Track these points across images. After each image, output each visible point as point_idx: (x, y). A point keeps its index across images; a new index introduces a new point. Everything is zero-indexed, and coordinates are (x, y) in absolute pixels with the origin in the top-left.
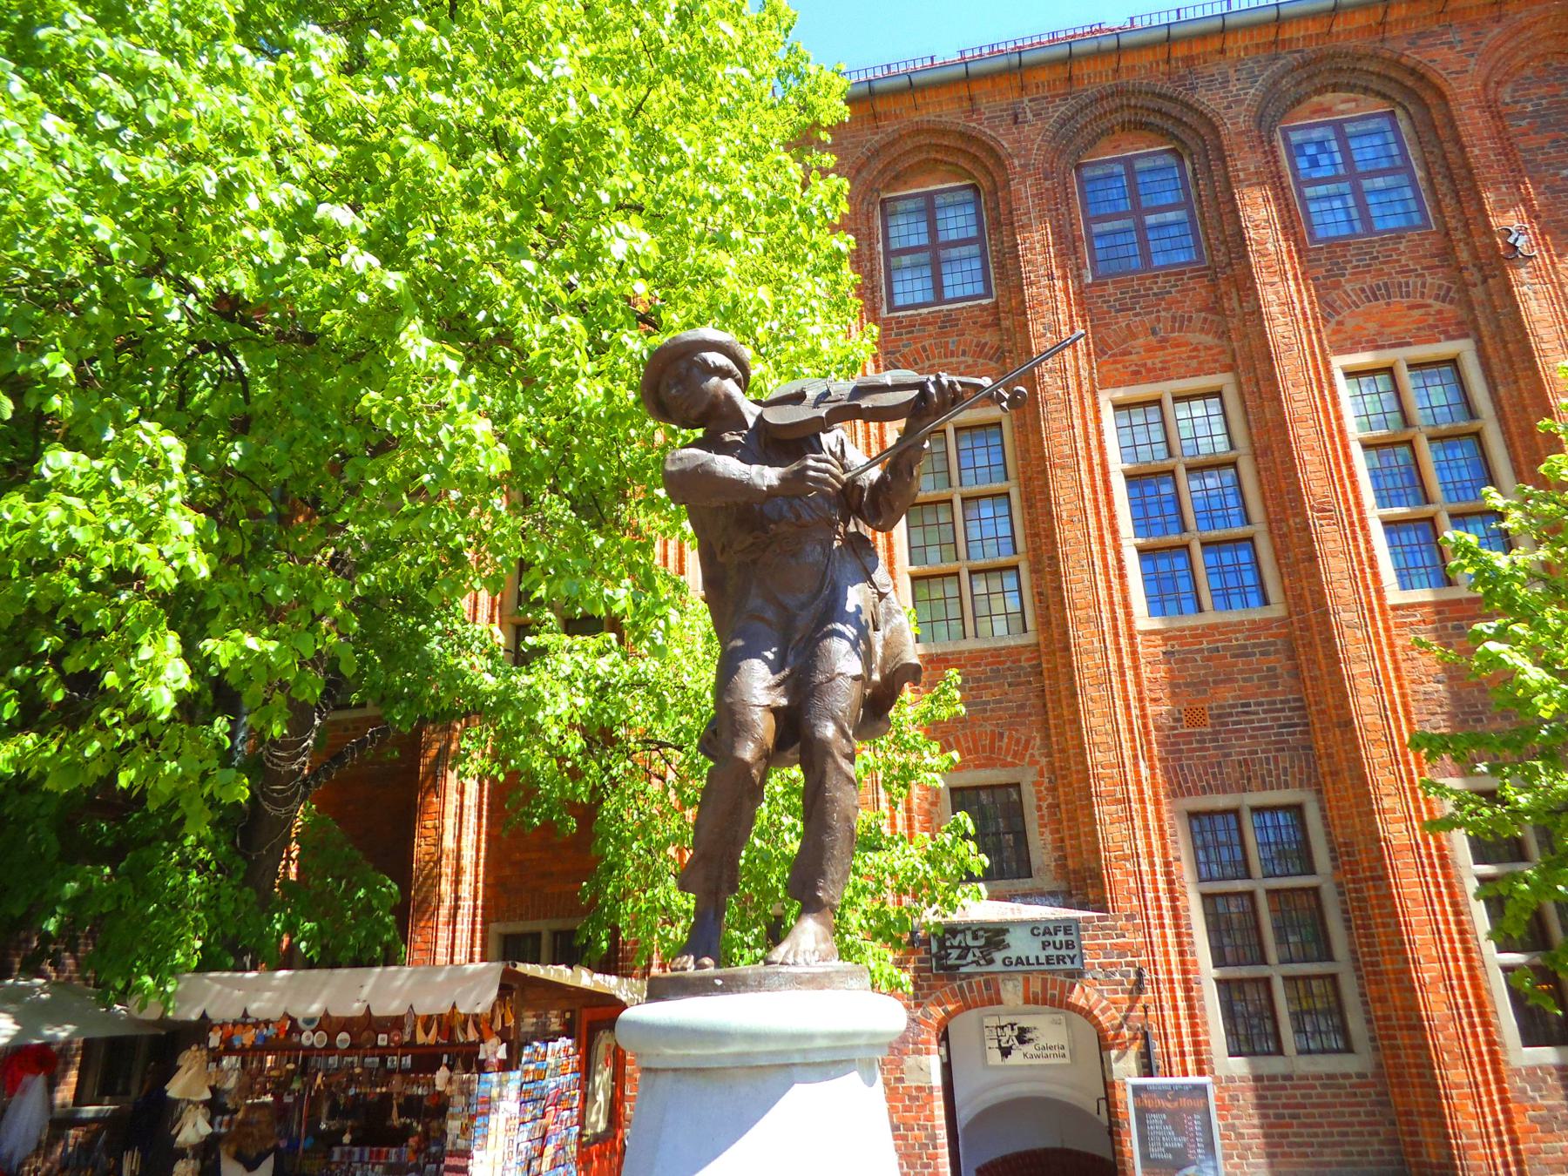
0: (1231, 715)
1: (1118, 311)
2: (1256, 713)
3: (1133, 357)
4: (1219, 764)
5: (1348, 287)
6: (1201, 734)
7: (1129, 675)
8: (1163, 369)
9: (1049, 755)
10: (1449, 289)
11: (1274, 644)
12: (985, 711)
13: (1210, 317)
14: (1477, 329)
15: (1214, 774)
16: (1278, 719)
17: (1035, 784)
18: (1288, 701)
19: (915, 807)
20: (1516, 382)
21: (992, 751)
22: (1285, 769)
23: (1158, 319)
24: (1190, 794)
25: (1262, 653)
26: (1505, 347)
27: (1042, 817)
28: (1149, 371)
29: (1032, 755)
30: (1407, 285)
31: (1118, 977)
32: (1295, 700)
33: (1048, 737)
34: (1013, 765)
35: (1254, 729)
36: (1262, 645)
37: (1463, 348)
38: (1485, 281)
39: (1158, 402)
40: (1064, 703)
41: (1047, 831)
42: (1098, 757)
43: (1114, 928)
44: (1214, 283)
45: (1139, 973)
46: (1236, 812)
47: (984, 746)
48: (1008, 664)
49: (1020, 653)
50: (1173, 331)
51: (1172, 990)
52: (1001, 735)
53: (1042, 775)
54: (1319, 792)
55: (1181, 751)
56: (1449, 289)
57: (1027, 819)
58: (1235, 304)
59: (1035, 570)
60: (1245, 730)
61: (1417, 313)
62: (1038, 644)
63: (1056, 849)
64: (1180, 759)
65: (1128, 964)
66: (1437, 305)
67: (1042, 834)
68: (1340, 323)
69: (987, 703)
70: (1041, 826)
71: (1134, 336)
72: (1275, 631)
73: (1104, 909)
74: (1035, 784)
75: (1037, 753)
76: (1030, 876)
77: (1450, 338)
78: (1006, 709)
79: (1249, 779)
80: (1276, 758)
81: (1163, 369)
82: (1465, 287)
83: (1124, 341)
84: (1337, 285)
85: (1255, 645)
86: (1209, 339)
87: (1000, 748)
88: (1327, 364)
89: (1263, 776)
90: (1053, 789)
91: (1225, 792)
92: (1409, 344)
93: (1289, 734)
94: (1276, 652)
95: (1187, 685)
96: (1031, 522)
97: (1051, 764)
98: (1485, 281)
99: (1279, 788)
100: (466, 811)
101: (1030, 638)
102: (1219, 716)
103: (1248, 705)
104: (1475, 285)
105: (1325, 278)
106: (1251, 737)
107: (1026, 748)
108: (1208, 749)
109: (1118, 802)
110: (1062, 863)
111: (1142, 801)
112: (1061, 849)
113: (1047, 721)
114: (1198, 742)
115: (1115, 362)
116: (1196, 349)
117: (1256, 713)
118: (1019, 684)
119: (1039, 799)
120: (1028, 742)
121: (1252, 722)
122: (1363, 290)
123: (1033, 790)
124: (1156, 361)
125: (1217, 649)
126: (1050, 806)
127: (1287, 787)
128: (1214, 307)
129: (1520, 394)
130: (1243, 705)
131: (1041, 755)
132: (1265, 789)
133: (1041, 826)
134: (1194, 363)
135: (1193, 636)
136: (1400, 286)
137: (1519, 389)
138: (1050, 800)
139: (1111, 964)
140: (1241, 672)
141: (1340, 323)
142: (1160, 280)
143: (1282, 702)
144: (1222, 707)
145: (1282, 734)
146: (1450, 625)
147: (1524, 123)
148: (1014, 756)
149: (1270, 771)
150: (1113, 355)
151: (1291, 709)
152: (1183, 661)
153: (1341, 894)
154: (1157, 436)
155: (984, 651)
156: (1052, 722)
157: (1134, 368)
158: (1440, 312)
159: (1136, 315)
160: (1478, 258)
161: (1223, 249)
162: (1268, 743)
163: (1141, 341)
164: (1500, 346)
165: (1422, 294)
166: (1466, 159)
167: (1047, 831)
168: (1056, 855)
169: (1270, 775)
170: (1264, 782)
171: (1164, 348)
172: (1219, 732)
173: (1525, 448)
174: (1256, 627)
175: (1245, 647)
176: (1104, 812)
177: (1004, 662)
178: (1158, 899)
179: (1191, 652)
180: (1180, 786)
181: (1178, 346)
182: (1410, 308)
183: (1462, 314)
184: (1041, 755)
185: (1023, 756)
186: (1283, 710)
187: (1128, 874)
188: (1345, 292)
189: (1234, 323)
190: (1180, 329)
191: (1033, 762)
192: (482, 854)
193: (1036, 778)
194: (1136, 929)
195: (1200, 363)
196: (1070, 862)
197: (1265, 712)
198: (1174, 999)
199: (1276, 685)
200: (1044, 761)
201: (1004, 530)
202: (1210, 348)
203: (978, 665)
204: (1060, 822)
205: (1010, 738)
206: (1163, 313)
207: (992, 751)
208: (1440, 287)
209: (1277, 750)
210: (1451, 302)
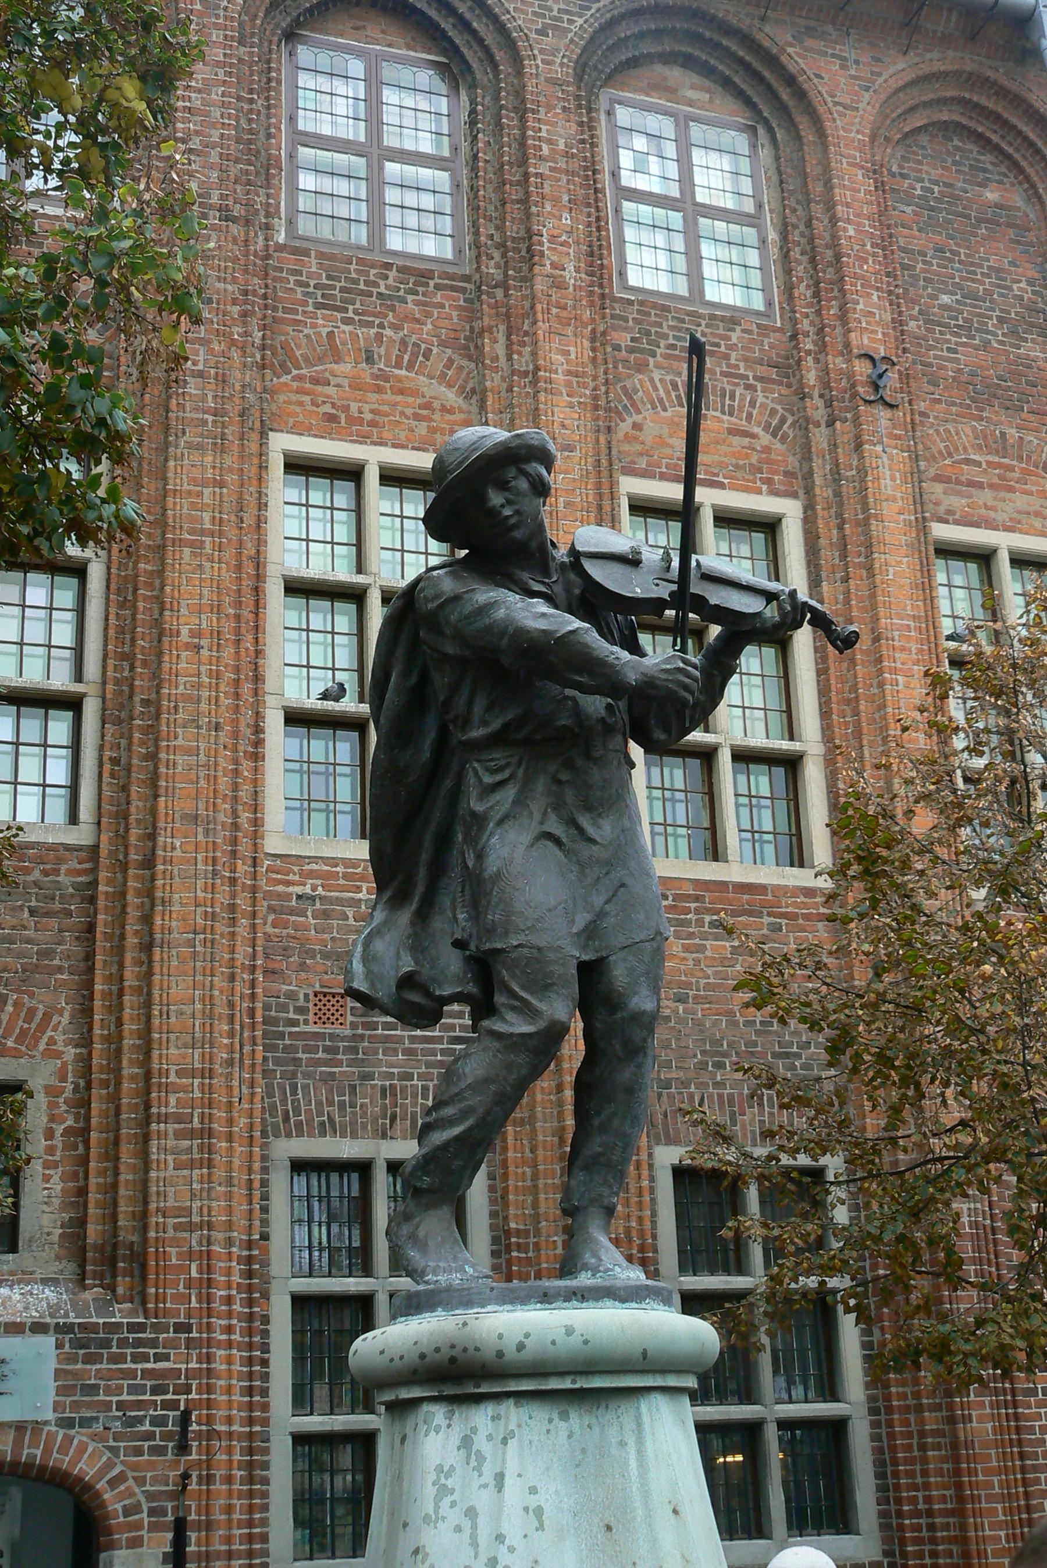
1: (318, 306)
3: (330, 390)
4: (353, 1088)
5: (657, 375)
6: (333, 1037)
8: (372, 424)
10: (783, 420)
13: (460, 361)
14: (809, 491)
15: (342, 1104)
17: (52, 1092)
20: (846, 580)
23: (379, 337)
24: (300, 1134)
26: (840, 527)
27: (50, 1150)
28: (352, 420)
29: (52, 1041)
30: (732, 397)
31: (147, 1427)
34: (17, 1055)
37: (790, 511)
38: (831, 423)
39: (353, 473)
40: (129, 956)
42: (172, 1055)
43: (153, 1343)
44: (471, 312)
45: (185, 1419)
46: (363, 1168)
48: (36, 875)
49: (60, 860)
50: (398, 365)
53: (63, 1079)
55: (297, 1062)
56: (783, 420)
58: (500, 350)
60: (399, 1040)
61: (737, 441)
62: (95, 849)
63: (64, 1206)
64: (294, 1075)
66: (765, 439)
67: (47, 1178)
68: (636, 426)
71: (338, 360)
75: (60, 1038)
76: (13, 1249)
77: (774, 492)
78: (21, 955)
81: (372, 424)
82: (804, 424)
83: (321, 360)
84: (642, 367)
86: (452, 397)
88: (613, 484)
91: (354, 1136)
92: (721, 486)
95: (326, 956)
96: (120, 630)
98: (831, 423)
101: (81, 835)
104: (818, 425)
105: (631, 350)
106: (407, 1052)
107: (42, 1028)
108: (339, 1064)
109: (192, 1134)
113: (89, 985)
114: (326, 1049)
115: (300, 391)
116: (427, 406)
118: (48, 914)
119: (52, 1119)
120: (47, 1017)
122: (675, 386)
124: (363, 407)
126: (67, 1132)
128: (471, 348)
129: (847, 601)
134: (422, 428)
135: (346, 876)
136: (723, 395)
137: (847, 593)
138: (70, 1122)
139: (139, 1405)
141: (636, 426)
142: (392, 274)
146: (707, 918)
147: (909, 210)
148: (19, 1040)
150: (300, 378)
152: (326, 915)
154: (343, 533)
156: (98, 987)
157: (327, 408)
158: (767, 449)
159: (347, 321)
160: (827, 385)
161: (497, 255)
162: (429, 1065)
163: (345, 368)
164: (834, 522)
165: (750, 416)
166: (835, 237)
167: (56, 1174)
171: (379, 390)
172: (362, 1037)
173: (842, 679)
176: (168, 1147)
177: (28, 871)
179: (339, 901)
180: (286, 1119)
181: (402, 392)
182: (731, 432)
183: (793, 462)
185: (37, 1040)
187: (190, 1255)
188: (652, 380)
189: (493, 381)
190: (410, 367)
191: (52, 1053)
193: (54, 1081)
195: (433, 430)
200: (71, 1053)
201: (64, 634)
202: (451, 411)
204: (84, 1161)
205: (17, 1004)
206: (388, 332)
208: (773, 412)
210: (783, 439)
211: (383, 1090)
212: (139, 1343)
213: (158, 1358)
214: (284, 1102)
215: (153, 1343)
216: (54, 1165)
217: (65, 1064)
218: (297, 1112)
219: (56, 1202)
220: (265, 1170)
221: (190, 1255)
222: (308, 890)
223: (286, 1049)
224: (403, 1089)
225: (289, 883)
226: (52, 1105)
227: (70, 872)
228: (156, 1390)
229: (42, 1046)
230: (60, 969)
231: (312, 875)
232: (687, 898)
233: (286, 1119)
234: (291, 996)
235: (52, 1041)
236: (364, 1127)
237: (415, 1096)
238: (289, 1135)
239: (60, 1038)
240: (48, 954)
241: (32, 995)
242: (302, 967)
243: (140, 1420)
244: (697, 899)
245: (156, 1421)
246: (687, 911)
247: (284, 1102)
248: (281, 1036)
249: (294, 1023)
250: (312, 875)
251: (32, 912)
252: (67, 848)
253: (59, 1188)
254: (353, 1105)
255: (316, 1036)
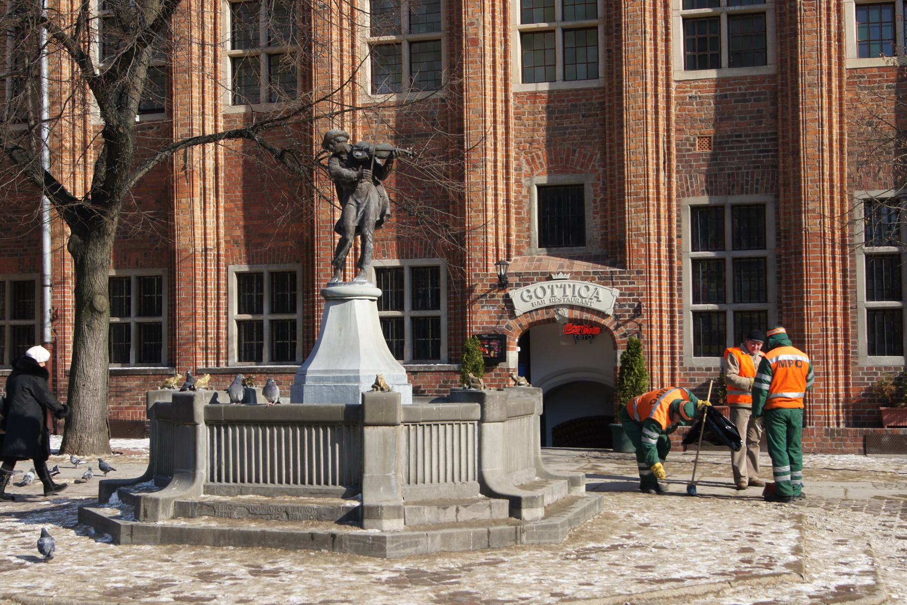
0: (728, 142)
2: (744, 142)
4: (716, 175)
7: (662, 113)
9: (604, 166)
11: (765, 93)
12: (565, 133)
16: (759, 146)
17: (593, 185)
18: (766, 134)
19: (512, 199)
21: (567, 162)
22: (758, 180)
25: (756, 100)
27: (596, 207)
29: (594, 166)
31: (627, 308)
32: (772, 134)
33: (605, 153)
34: (581, 172)
35: (741, 153)
36: (757, 94)
41: (598, 216)
43: (629, 278)
45: (639, 306)
47: (562, 159)
48: (584, 101)
51: (661, 316)
52: (574, 151)
54: (777, 196)
55: (691, 166)
57: (586, 208)
59: (607, 33)
60: (735, 153)
62: (604, 88)
63: (602, 228)
65: (634, 300)
67: (595, 218)
69: (567, 128)
70: (594, 213)
72: (766, 84)
73: (624, 267)
74: (593, 185)
75: (597, 164)
79: (733, 186)
80: (753, 172)
85: (752, 94)
87: (573, 160)
89: (742, 184)
90: (604, 189)
93: (764, 157)
94: (765, 99)
97: (605, 172)
99: (751, 193)
100: (207, 192)
102: (720, 143)
103: (740, 136)
106: (739, 158)
107: (590, 161)
109: (637, 200)
110: (604, 239)
111: (658, 199)
112: (606, 228)
113: (604, 143)
117: (744, 142)
118: (589, 116)
119: (595, 196)
120: (591, 156)
121: (741, 147)
123: (591, 189)
125: (726, 96)
126: (601, 200)
127: (757, 193)
130: (737, 136)
131: (599, 166)
132: (742, 193)
133: (594, 213)
138: (602, 196)
140: (740, 112)
143: (763, 135)
144: (723, 137)
145: (759, 157)
148: (582, 166)
149: (747, 182)
151: (768, 140)
153: (779, 262)
155: (567, 91)
156: (607, 144)
167: (598, 216)
168: (602, 232)
169: (747, 185)
170: (742, 188)
172: (719, 154)
174: (754, 80)
175: (744, 95)
176: (630, 205)
177: (580, 100)
178: (659, 262)
184: (599, 166)
185: (588, 166)
186: (763, 140)
187: (642, 245)
191: (594, 171)
192: (222, 221)
194: (642, 278)
196: (609, 237)
197: (751, 141)
198: (661, 321)
199: (761, 123)
203: (563, 101)
205: (580, 153)
207: (567, 162)
209: (755, 167)
211: (729, 175)
212: (622, 278)
213: (630, 283)
214: (687, 182)
215: (629, 278)
216: (597, 213)
217: (599, 175)
218: (692, 187)
219: (599, 227)
220: (679, 210)
221: (642, 245)
222: (694, 94)
223: (686, 161)
224: (738, 174)
225: (685, 92)
226: (595, 191)
227: (596, 99)
228: (630, 295)
229: (590, 168)
230: (595, 138)
231: (696, 87)
232: (874, 76)
233: (688, 190)
234: (687, 139)
235: (594, 166)
236: (721, 190)
237: (743, 176)
238: (688, 196)
239: (597, 164)
240: (590, 132)
241: (585, 149)
242: (692, 127)
243: (624, 305)
244: (880, 76)
245: (630, 306)
246: (875, 82)
247: (687, 182)
248: (684, 156)
249: (689, 150)
250: (696, 87)
251: (583, 116)
252: (595, 89)
253: (599, 221)
254: (716, 182)
255: (699, 155)
